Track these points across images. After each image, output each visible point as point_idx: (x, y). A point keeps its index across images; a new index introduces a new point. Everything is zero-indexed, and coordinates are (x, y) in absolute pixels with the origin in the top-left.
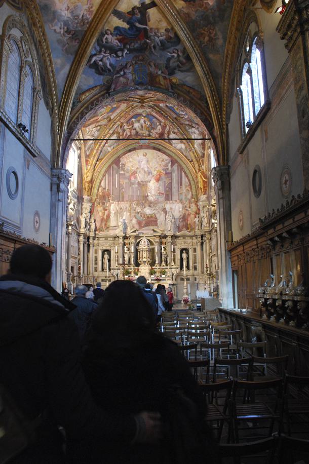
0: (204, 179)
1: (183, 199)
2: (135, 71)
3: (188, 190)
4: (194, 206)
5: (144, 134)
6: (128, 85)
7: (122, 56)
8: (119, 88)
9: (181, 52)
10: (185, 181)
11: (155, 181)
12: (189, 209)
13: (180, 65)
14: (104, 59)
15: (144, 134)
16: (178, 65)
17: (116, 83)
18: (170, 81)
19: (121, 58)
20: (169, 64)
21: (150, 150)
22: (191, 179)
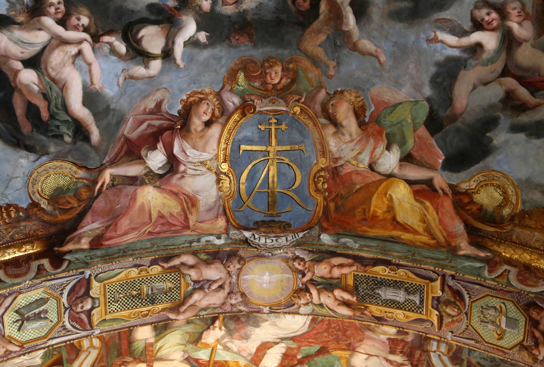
2: (236, 160)
6: (187, 227)
7: (167, 54)
8: (131, 237)
9: (525, 15)
13: (523, 92)
14: (57, 58)
16: (509, 97)
17: (113, 217)
18: (462, 201)
19: (156, 65)
20: (449, 100)
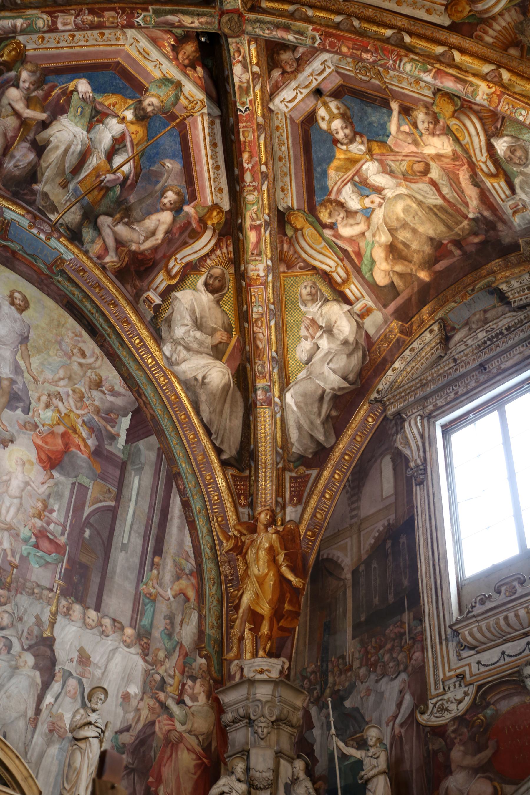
0: (291, 577)
1: (157, 634)
3: (187, 600)
4: (202, 699)
5: (54, 209)
10: (181, 544)
11: (33, 456)
12: (175, 709)
15: (54, 209)
21: (50, 303)
22: (207, 551)
